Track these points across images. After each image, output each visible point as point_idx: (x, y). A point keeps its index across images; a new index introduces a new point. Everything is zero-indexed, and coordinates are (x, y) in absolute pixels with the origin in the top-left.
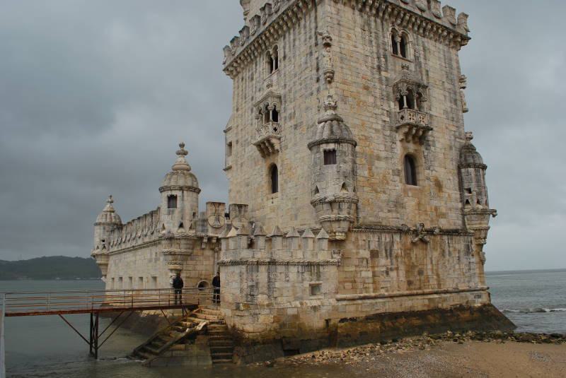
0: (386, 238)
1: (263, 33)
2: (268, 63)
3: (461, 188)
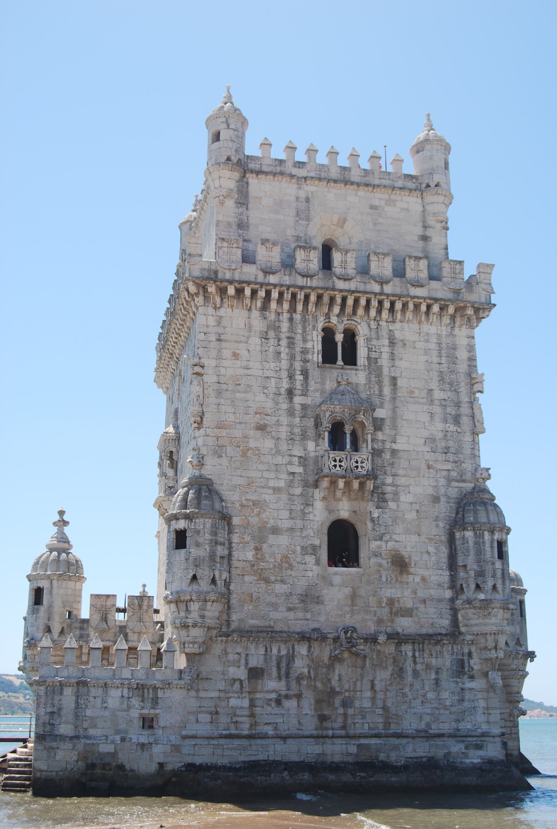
3: (452, 564)
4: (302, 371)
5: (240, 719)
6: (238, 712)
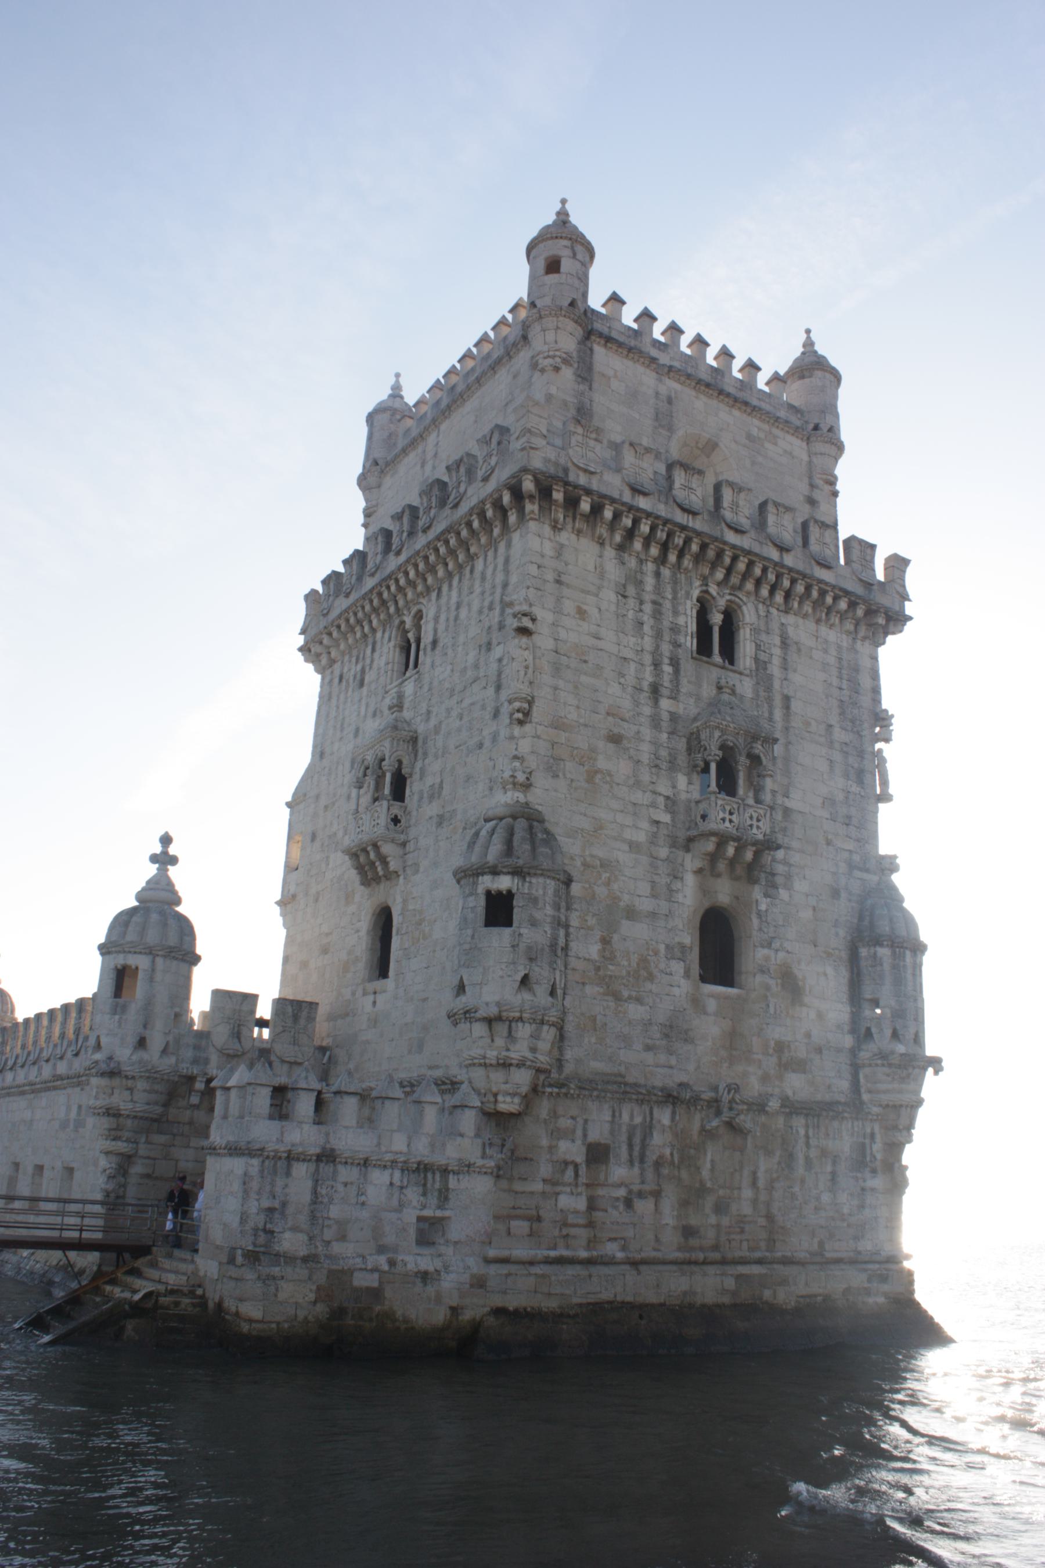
0: (631, 1115)
2: (402, 648)
4: (671, 659)
5: (573, 1231)
6: (571, 1219)
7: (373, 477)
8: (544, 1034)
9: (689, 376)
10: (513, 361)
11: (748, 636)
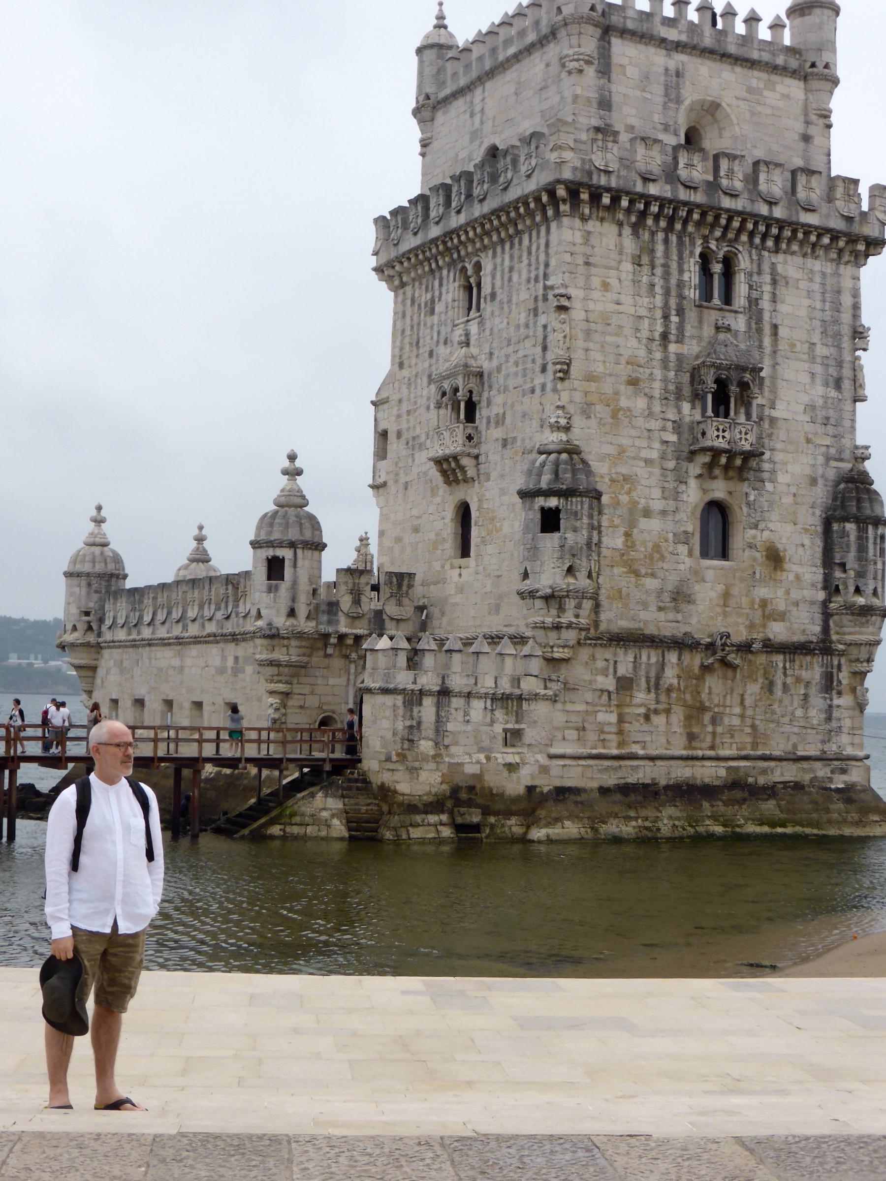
0: (650, 657)
1: (456, 231)
3: (828, 561)
5: (608, 737)
6: (606, 729)
7: (427, 109)
8: (584, 606)
9: (694, 48)
10: (545, 49)
11: (743, 279)
